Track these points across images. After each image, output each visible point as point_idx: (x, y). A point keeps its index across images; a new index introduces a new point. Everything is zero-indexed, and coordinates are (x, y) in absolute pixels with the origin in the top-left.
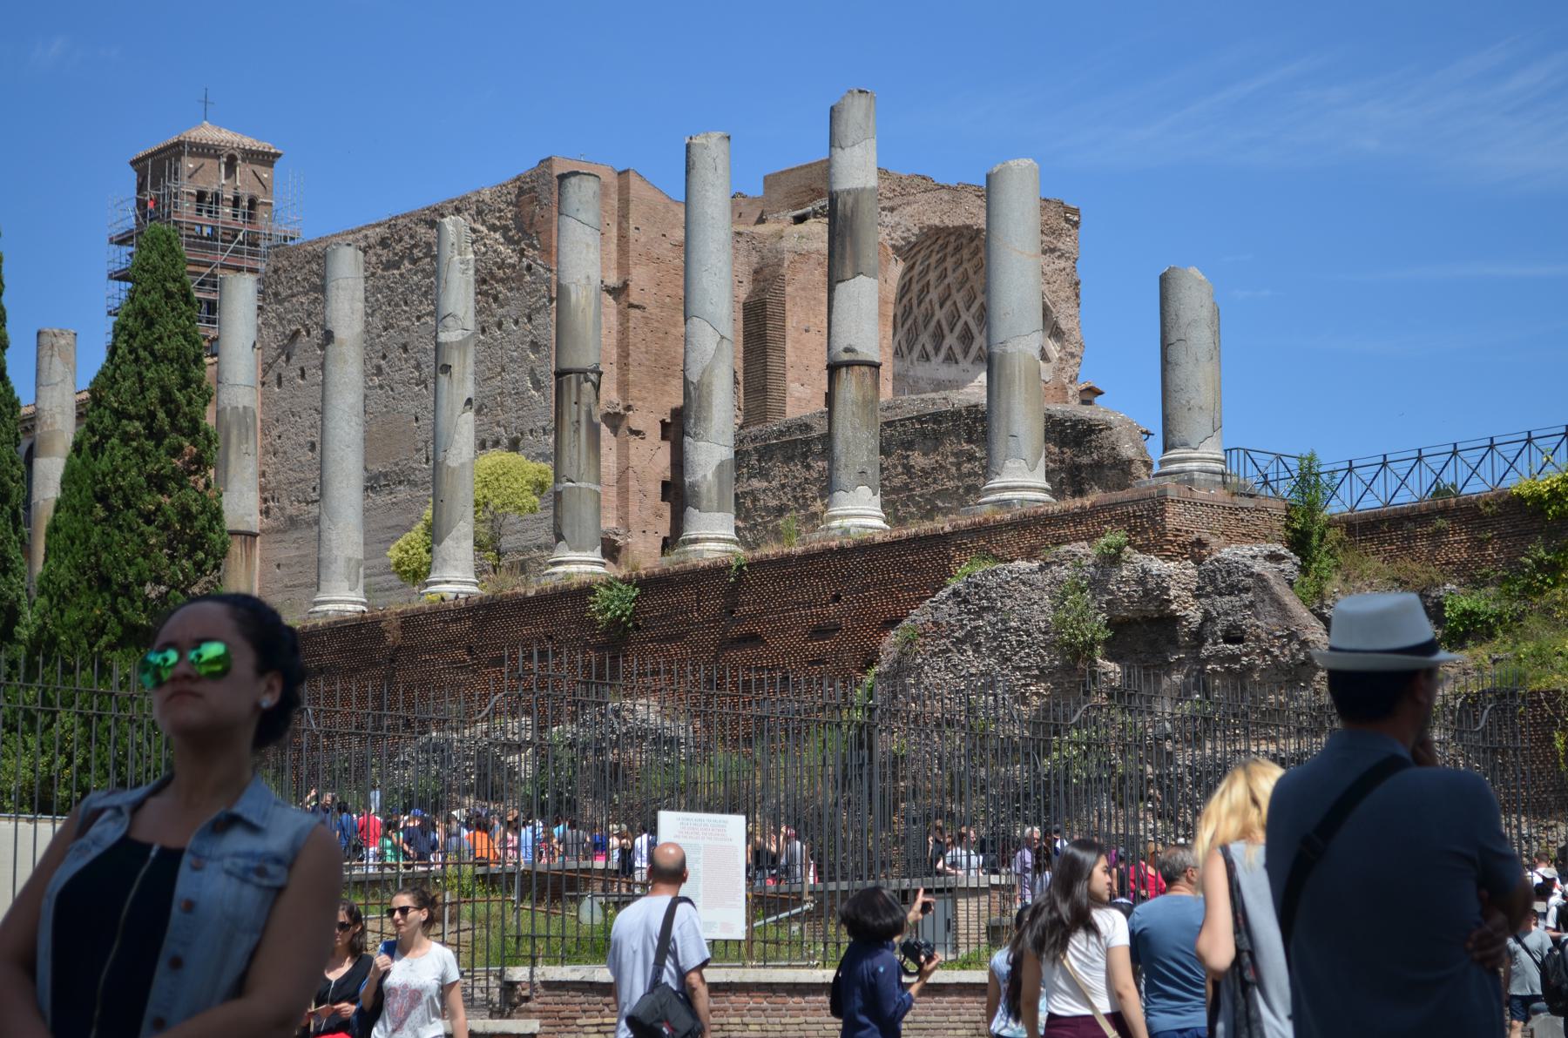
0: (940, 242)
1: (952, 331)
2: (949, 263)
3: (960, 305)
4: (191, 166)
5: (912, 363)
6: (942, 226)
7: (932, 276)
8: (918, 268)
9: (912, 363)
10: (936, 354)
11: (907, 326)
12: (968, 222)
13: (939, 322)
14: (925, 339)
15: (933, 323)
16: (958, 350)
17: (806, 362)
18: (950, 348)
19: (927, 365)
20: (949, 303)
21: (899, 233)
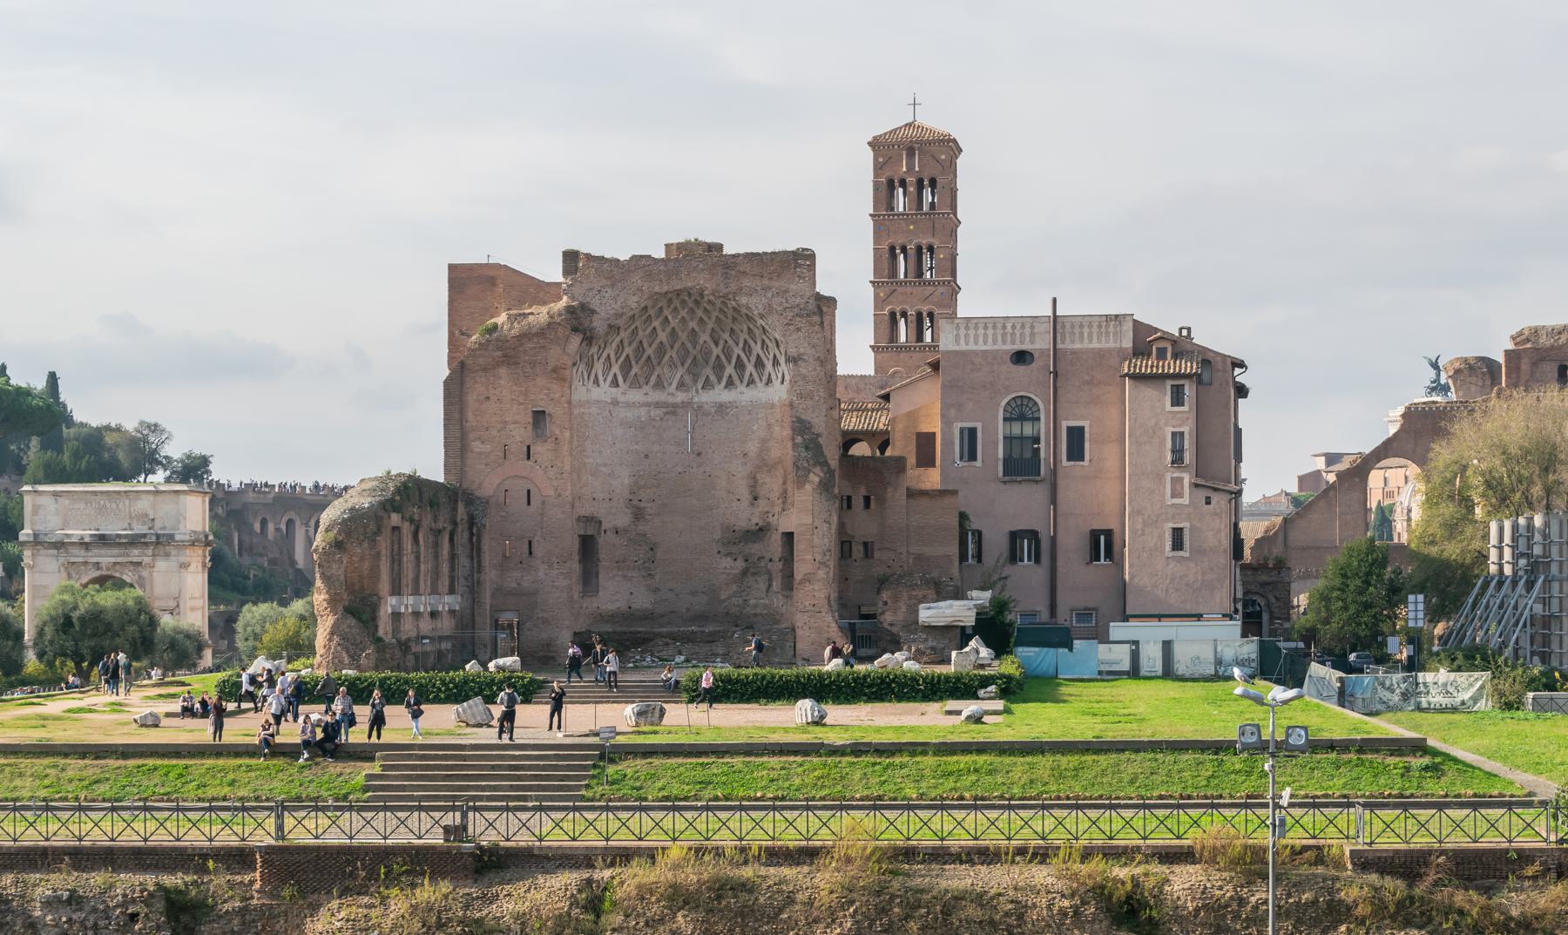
0: (676, 303)
1: (730, 362)
2: (700, 313)
3: (731, 342)
4: (881, 160)
5: (697, 391)
6: (663, 291)
7: (693, 324)
8: (674, 322)
9: (697, 391)
10: (719, 381)
11: (687, 365)
12: (689, 284)
13: (718, 357)
14: (708, 371)
15: (713, 359)
16: (735, 377)
17: (486, 425)
18: (730, 376)
19: (711, 392)
20: (722, 342)
21: (619, 303)
